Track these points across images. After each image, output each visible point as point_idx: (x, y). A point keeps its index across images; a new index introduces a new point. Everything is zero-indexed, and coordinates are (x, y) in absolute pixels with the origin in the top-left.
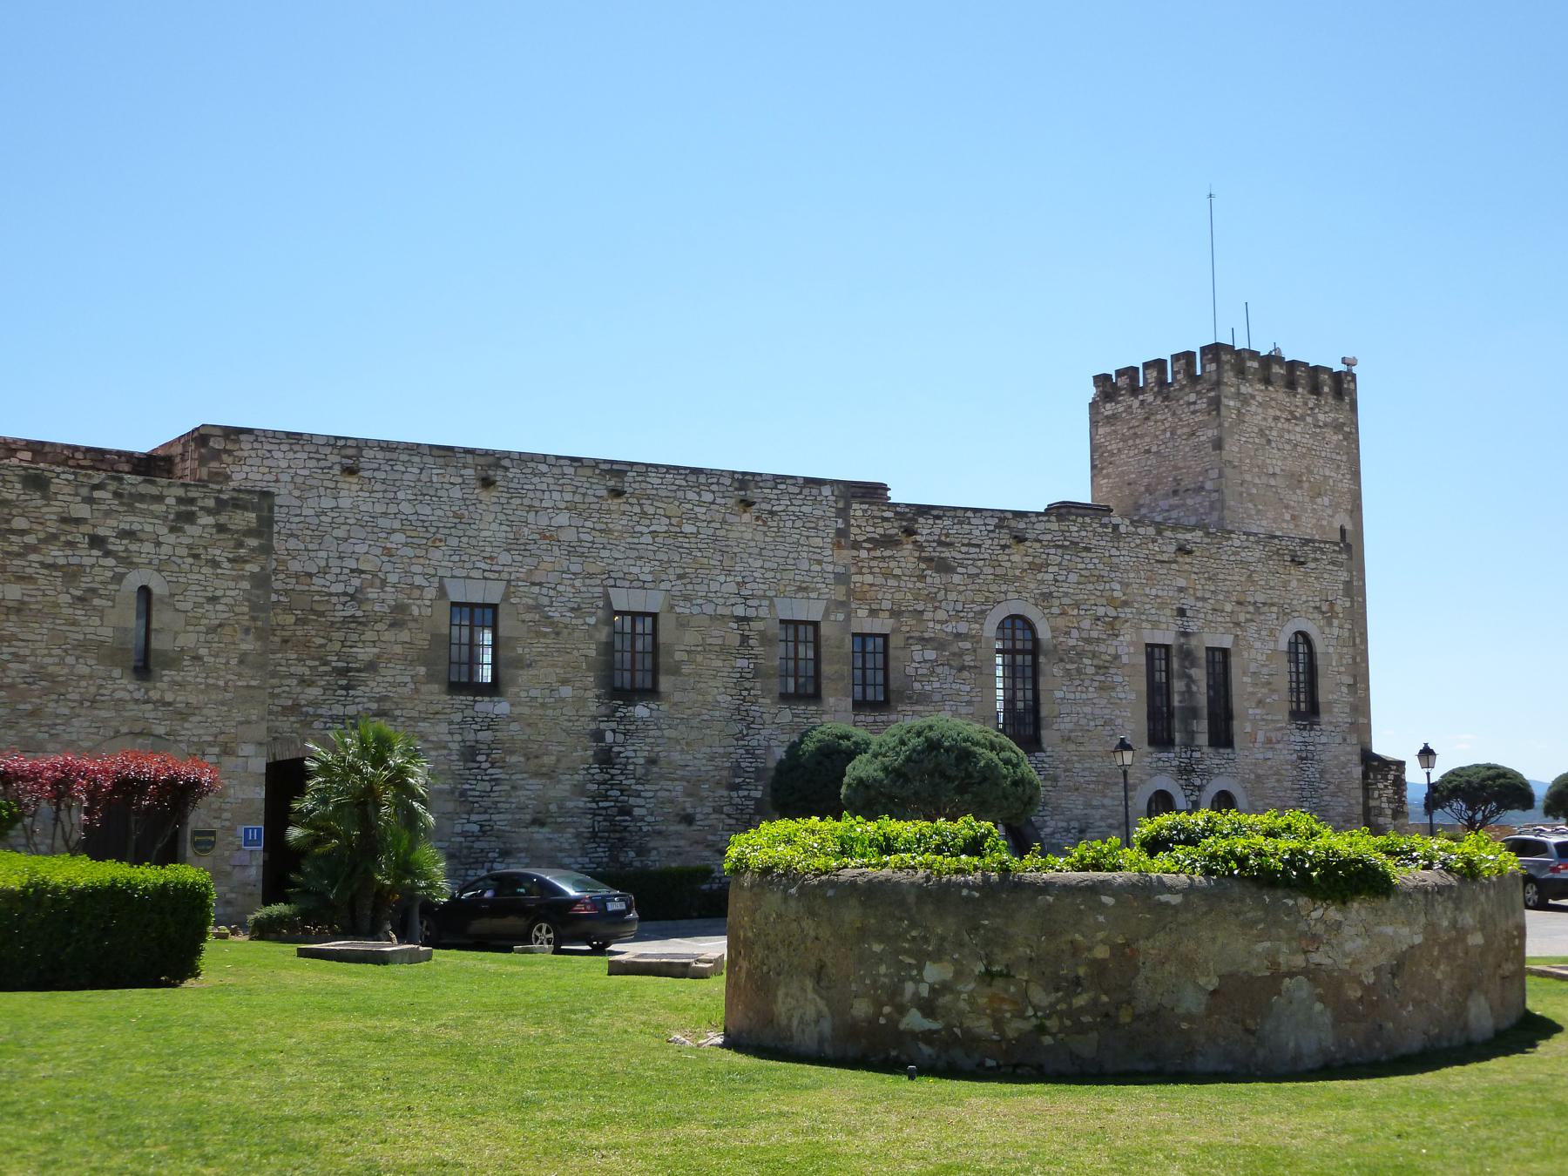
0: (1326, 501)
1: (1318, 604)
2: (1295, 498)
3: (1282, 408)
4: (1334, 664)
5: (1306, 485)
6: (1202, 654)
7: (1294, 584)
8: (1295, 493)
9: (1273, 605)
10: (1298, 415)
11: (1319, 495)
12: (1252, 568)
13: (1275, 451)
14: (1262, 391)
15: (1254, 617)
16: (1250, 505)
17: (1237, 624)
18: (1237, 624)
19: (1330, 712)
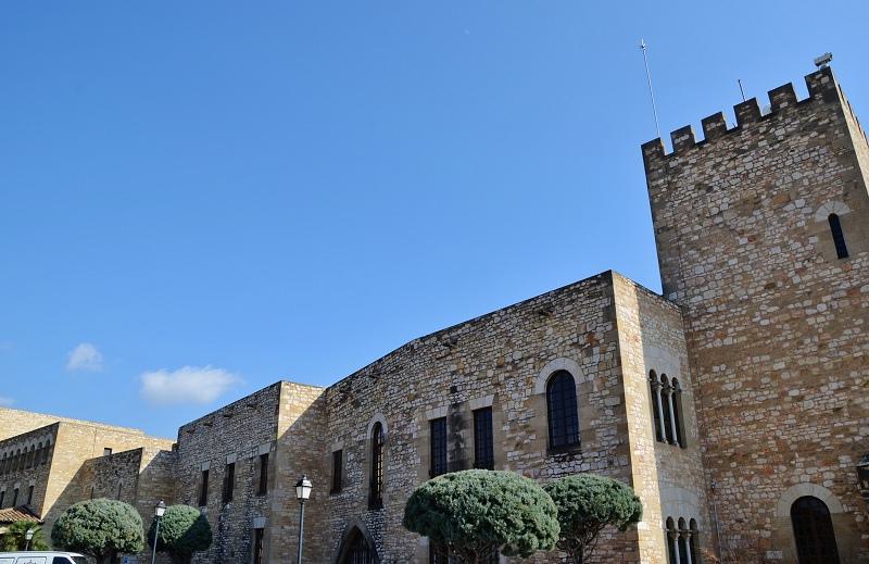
0: (800, 203)
1: (575, 340)
2: (753, 220)
3: (724, 153)
4: (596, 389)
5: (766, 203)
6: (470, 417)
7: (550, 331)
8: (751, 215)
9: (529, 357)
10: (746, 148)
11: (789, 201)
12: (510, 334)
13: (720, 192)
14: (696, 153)
15: (512, 374)
16: (692, 252)
17: (498, 384)
18: (498, 384)
19: (593, 438)
